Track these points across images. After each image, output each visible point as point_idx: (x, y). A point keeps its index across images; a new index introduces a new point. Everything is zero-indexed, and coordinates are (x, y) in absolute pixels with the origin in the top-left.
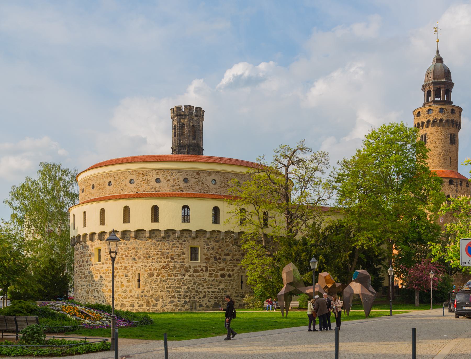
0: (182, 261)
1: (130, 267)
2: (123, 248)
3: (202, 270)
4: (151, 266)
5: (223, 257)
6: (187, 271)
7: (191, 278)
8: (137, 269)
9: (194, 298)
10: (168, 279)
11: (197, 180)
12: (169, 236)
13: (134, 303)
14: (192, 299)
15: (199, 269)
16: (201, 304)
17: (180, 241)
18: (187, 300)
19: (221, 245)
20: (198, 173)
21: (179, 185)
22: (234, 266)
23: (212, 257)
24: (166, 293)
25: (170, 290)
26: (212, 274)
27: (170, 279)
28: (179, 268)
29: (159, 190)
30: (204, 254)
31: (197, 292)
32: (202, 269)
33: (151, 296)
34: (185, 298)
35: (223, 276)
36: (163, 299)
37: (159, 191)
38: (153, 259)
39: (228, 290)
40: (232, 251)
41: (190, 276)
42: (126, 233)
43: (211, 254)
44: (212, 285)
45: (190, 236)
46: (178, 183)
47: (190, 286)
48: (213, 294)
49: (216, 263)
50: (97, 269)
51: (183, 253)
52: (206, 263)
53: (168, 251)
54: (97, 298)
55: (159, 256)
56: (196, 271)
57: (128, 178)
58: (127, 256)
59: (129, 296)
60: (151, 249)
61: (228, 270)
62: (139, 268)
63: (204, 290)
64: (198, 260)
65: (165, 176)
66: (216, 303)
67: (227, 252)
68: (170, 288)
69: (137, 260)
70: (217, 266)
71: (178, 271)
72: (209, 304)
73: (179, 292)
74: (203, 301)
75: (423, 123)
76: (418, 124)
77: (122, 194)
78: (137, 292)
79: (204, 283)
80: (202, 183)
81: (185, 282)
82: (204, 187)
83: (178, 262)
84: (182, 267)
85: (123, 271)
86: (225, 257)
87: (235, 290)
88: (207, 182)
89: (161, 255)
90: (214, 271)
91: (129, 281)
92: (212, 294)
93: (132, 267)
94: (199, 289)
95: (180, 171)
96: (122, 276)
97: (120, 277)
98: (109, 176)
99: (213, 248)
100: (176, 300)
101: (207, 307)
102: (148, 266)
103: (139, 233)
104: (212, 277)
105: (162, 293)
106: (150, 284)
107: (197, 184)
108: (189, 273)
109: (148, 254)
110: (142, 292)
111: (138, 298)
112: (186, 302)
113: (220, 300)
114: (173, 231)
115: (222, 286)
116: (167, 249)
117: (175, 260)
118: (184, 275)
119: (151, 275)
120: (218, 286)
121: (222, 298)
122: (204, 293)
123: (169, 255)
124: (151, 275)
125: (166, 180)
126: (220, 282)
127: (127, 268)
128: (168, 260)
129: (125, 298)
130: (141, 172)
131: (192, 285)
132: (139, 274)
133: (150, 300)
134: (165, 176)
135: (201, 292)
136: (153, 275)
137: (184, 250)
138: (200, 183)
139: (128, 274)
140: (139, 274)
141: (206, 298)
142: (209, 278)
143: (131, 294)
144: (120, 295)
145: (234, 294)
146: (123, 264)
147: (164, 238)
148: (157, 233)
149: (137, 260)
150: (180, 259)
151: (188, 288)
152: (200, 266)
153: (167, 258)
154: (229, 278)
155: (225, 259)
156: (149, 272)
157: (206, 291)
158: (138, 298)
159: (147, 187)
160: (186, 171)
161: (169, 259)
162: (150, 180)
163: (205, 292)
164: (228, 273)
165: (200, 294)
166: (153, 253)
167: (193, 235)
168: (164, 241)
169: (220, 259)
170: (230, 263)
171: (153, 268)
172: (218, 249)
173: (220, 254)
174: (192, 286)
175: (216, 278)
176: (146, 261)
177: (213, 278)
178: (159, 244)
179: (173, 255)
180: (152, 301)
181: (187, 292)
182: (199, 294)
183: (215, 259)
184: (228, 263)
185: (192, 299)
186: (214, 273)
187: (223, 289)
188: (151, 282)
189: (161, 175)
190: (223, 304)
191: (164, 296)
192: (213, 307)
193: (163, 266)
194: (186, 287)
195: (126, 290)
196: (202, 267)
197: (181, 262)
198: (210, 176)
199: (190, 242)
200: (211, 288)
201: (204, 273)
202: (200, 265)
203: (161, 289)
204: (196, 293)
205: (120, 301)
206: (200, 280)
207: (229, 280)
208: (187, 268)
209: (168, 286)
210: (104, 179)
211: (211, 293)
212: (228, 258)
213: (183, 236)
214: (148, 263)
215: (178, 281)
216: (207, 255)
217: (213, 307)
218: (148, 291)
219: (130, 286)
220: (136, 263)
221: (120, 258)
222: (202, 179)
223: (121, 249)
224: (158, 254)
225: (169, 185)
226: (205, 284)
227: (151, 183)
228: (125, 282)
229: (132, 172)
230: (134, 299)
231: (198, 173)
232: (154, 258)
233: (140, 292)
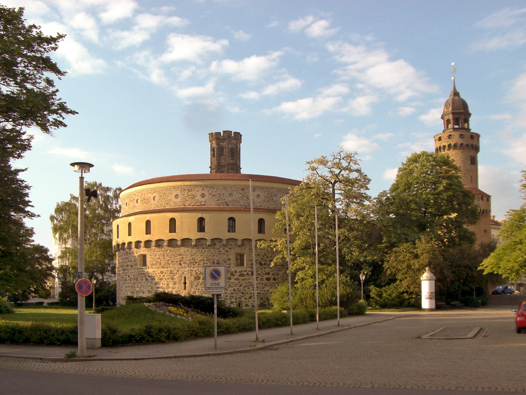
3: (248, 274)
6: (232, 275)
7: (237, 281)
9: (240, 298)
11: (241, 195)
12: (215, 244)
14: (238, 299)
15: (245, 273)
17: (226, 249)
18: (234, 300)
22: (279, 271)
31: (243, 293)
35: (268, 279)
37: (205, 205)
41: (236, 279)
45: (236, 245)
47: (236, 288)
51: (229, 259)
61: (273, 274)
70: (263, 271)
75: (444, 147)
76: (440, 147)
89: (207, 260)
90: (260, 275)
94: (245, 290)
103: (185, 242)
108: (235, 277)
109: (194, 260)
120: (263, 288)
126: (266, 285)
136: (200, 279)
137: (231, 257)
147: (209, 246)
148: (202, 242)
151: (234, 290)
152: (246, 271)
163: (251, 293)
169: (265, 264)
172: (263, 256)
174: (238, 288)
178: (205, 251)
185: (238, 299)
194: (232, 289)
199: (236, 249)
201: (250, 277)
204: (242, 295)
225: (215, 200)
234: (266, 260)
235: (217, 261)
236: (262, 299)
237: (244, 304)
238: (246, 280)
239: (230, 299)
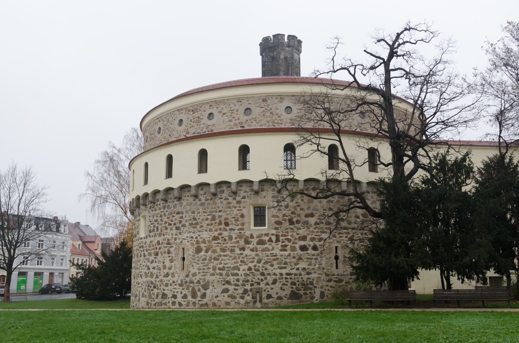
0: (240, 227)
1: (173, 240)
2: (167, 213)
3: (270, 240)
4: (199, 237)
5: (303, 219)
6: (247, 242)
7: (253, 254)
8: (181, 242)
10: (220, 256)
11: (263, 109)
13: (177, 292)
14: (256, 286)
15: (266, 238)
16: (269, 293)
17: (238, 198)
18: (248, 287)
19: (300, 201)
20: (264, 100)
21: (238, 119)
23: (285, 220)
24: (218, 277)
25: (224, 272)
26: (286, 246)
27: (225, 256)
28: (236, 238)
29: (213, 128)
30: (273, 216)
31: (262, 274)
32: (270, 238)
33: (199, 282)
34: (243, 285)
35: (304, 248)
36: (213, 286)
38: (202, 226)
39: (312, 271)
40: (317, 210)
42: (170, 192)
43: (284, 215)
44: (286, 263)
46: (236, 117)
47: (252, 265)
48: (288, 277)
49: (292, 229)
50: (142, 244)
51: (242, 216)
52: (276, 229)
53: (220, 214)
54: (140, 285)
55: (208, 222)
56: (261, 242)
57: (176, 119)
58: (170, 224)
59: (171, 282)
60: (199, 213)
61: (313, 239)
62: (184, 241)
63: (274, 271)
64: (265, 226)
65: (219, 109)
66: (293, 292)
67: (309, 212)
68: (223, 269)
69: (182, 228)
70: (295, 234)
71: (235, 243)
72: (282, 294)
73: (237, 275)
74: (272, 289)
78: (181, 276)
79: (274, 260)
80: (271, 113)
81: (245, 260)
82: (274, 118)
83: (234, 230)
84: (240, 237)
85: (166, 245)
86: (306, 219)
87: (325, 270)
88: (278, 111)
89: (211, 220)
90: (289, 240)
91: (171, 261)
92: (286, 278)
93: (176, 239)
94: (266, 269)
95: (239, 100)
96: (165, 252)
97: (162, 254)
98: (159, 121)
99: (287, 207)
100: (231, 288)
101: (279, 298)
102: (194, 237)
104: (286, 250)
105: (213, 278)
106: (198, 264)
107: (264, 115)
108: (251, 246)
109: (195, 219)
110: (187, 276)
111: (181, 285)
112: (246, 291)
113: (300, 287)
114: (227, 183)
115: (302, 265)
116: (220, 211)
117: (231, 227)
118: (243, 249)
119: (198, 250)
120: (296, 264)
121: (304, 285)
122: (274, 277)
123: (222, 219)
124: (198, 250)
125: (222, 114)
126: (300, 258)
127: (170, 241)
128: (220, 227)
129: (167, 285)
130: (191, 108)
131: (255, 263)
132: (183, 249)
133: (197, 289)
134: (219, 109)
135: (269, 274)
137: (244, 211)
138: (268, 114)
139: (171, 249)
140: (183, 249)
141: (278, 283)
142: (282, 253)
143: (173, 279)
144: (161, 281)
145: (323, 277)
146: (166, 236)
148: (206, 188)
149: (182, 228)
150: (237, 225)
151: (250, 269)
152: (267, 235)
153: (220, 223)
154: (314, 252)
155: (306, 223)
156: (196, 246)
157: (278, 273)
158: (181, 285)
159: (198, 127)
160: (248, 98)
161: (223, 226)
162: (201, 117)
164: (312, 244)
165: (268, 277)
166: (201, 218)
167: (256, 187)
168: (215, 199)
169: (298, 222)
170: (315, 228)
171: (201, 240)
172: (295, 208)
173: (299, 215)
174: (255, 266)
175: (292, 253)
176: (192, 230)
177: (287, 253)
179: (228, 219)
180: (199, 290)
181: (248, 275)
182: (266, 278)
183: (291, 222)
184: (311, 229)
185: (256, 286)
186: (290, 244)
187: (304, 269)
188: (198, 260)
189: (215, 108)
190: (305, 294)
191: (216, 281)
192: (289, 299)
193: (214, 236)
194: (246, 267)
195: (168, 273)
196: (270, 236)
197: (239, 230)
198: (282, 102)
200: (285, 268)
201: (274, 244)
202: (267, 232)
203: (211, 271)
204: (261, 277)
205: (162, 290)
206: (268, 256)
207: (313, 255)
208: (247, 237)
209: (221, 266)
211: (284, 276)
212: (312, 221)
213: (241, 190)
214: (194, 233)
215: (235, 258)
216: (278, 217)
217: (289, 299)
218: (194, 275)
219: (173, 268)
220: (180, 233)
221: (163, 228)
222: (271, 107)
224: (207, 219)
226: (275, 263)
227: (202, 122)
228: (168, 264)
230: (177, 287)
231: (264, 100)
232: (203, 224)
233: (185, 275)
234: (299, 215)
235: (226, 219)
236: (294, 284)
237: (264, 295)
238: (269, 250)
239: (243, 285)
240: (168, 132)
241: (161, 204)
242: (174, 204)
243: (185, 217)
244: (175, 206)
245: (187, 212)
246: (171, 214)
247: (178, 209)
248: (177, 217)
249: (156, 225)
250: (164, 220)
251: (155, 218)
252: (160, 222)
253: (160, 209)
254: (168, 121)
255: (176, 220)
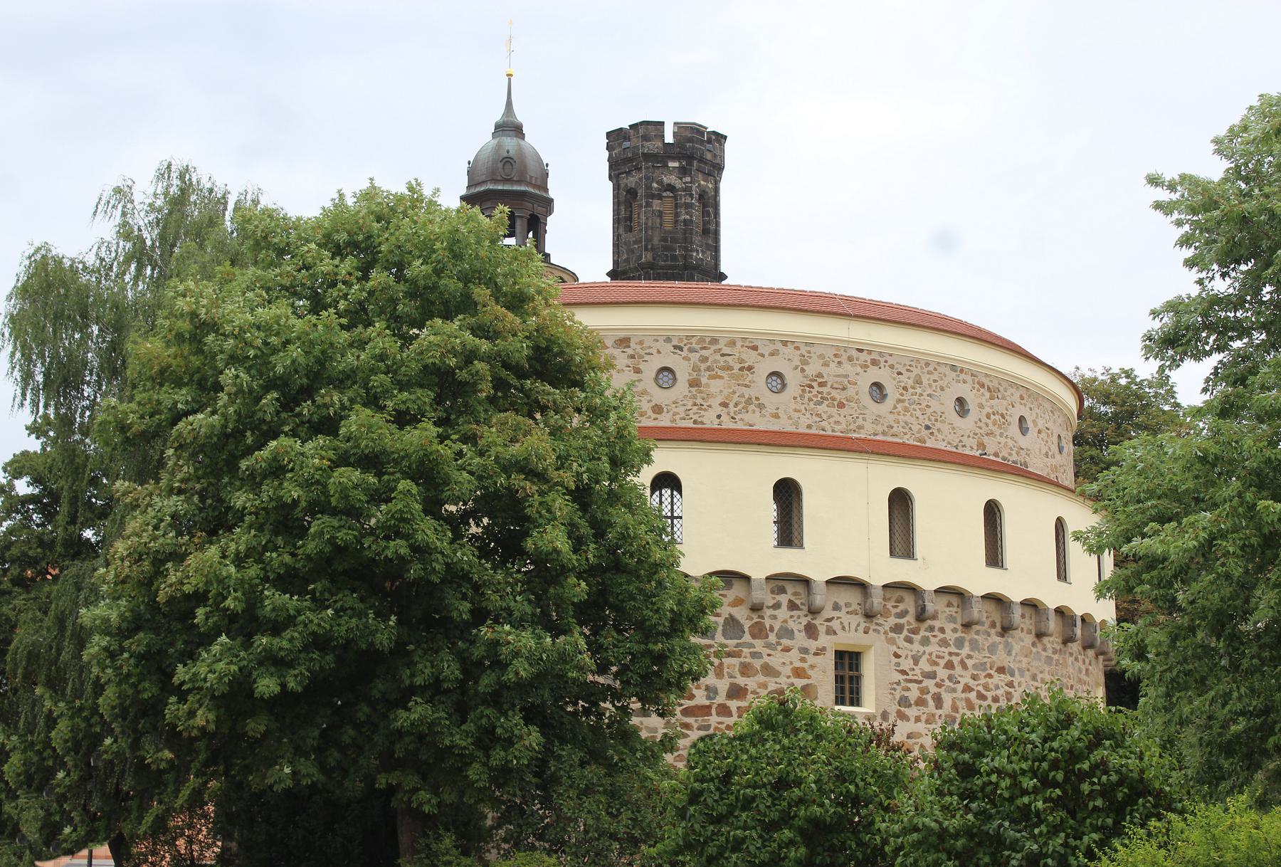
2: (969, 663)
77: (928, 445)
130: (986, 381)
210: (847, 368)
223: (965, 666)
229: (962, 371)
240: (918, 413)
241: (948, 631)
242: (990, 640)
243: (1020, 684)
244: (992, 649)
245: (1022, 672)
246: (982, 666)
247: (1001, 658)
248: (998, 679)
249: (934, 690)
250: (963, 681)
251: (924, 665)
252: (947, 683)
253: (944, 643)
254: (919, 382)
255: (997, 687)
